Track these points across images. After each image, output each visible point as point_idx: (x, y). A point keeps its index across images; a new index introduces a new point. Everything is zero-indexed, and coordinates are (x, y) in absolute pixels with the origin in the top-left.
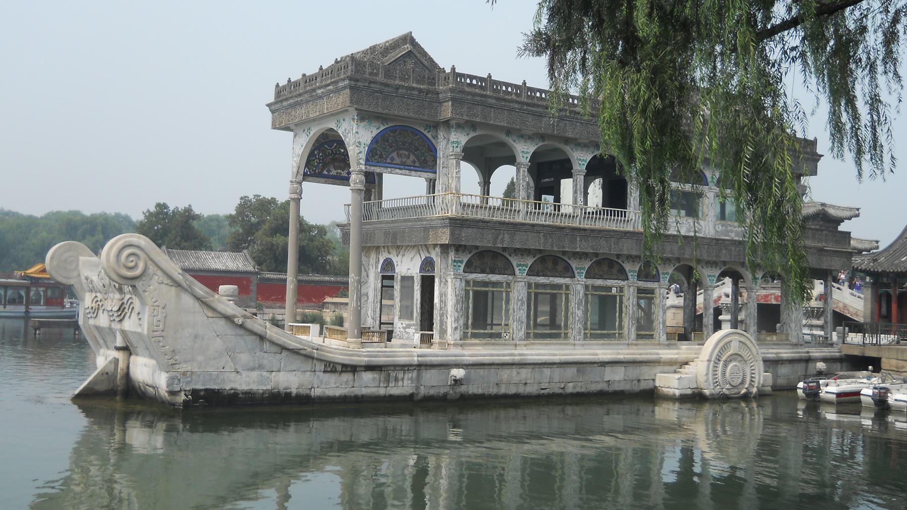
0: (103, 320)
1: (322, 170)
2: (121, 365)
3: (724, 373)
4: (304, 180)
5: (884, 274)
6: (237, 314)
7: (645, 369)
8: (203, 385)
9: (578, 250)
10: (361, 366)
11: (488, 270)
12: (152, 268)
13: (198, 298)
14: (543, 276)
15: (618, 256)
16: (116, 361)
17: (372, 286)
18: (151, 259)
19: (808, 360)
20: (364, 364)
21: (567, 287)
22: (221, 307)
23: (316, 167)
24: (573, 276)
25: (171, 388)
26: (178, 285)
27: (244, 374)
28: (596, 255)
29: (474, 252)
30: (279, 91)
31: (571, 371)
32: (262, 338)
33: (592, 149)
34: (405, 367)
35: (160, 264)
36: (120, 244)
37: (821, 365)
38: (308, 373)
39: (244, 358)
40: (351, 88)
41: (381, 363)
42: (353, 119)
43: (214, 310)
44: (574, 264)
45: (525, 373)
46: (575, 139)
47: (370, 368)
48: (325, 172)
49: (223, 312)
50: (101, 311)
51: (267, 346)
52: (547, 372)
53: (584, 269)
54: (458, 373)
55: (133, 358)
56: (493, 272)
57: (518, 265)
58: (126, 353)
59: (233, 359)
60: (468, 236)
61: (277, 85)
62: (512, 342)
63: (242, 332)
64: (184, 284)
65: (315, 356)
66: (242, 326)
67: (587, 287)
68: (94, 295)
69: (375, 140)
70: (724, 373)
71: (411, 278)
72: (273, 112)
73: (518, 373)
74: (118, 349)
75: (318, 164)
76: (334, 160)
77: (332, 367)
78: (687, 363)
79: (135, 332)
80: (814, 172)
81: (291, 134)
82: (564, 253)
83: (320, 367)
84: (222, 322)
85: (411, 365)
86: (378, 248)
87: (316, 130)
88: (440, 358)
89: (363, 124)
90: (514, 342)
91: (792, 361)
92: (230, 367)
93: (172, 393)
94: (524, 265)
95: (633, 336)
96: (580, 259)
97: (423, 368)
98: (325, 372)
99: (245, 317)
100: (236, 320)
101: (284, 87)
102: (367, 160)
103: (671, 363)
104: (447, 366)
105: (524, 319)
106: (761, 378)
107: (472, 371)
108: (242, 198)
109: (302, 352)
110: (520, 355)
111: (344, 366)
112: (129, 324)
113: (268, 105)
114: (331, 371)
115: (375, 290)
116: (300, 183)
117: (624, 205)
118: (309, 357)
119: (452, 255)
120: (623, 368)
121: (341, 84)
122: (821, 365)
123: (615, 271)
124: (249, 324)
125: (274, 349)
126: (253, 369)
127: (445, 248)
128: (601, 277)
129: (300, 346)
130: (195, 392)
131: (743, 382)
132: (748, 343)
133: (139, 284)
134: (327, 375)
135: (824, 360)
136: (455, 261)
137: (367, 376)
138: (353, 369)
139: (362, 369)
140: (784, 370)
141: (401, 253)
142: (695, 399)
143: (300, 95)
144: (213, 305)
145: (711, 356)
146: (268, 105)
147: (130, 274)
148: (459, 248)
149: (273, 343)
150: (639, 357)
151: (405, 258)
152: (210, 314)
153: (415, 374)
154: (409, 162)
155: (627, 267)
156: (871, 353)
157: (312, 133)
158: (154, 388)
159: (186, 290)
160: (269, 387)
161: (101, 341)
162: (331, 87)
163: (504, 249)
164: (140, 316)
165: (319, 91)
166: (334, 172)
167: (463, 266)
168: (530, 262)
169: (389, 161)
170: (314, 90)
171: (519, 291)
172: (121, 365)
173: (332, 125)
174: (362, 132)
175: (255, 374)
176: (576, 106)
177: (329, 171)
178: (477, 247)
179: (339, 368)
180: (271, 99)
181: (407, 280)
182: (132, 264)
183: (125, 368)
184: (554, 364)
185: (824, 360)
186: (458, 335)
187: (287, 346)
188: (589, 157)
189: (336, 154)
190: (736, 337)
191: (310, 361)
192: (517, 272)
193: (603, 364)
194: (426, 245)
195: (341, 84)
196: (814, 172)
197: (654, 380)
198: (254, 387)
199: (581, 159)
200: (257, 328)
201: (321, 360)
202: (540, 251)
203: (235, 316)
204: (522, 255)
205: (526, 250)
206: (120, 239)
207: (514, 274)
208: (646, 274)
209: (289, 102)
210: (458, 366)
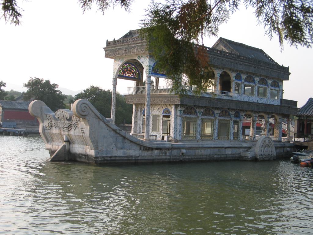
0: (55, 131)
1: (123, 74)
2: (67, 148)
3: (264, 151)
4: (118, 78)
5: (303, 116)
6: (117, 129)
7: (237, 150)
8: (106, 154)
10: (154, 148)
11: (189, 114)
12: (91, 112)
13: (105, 123)
14: (206, 116)
15: (229, 109)
16: (65, 146)
17: (139, 118)
18: (90, 109)
19: (284, 147)
20: (155, 147)
22: (112, 127)
23: (121, 73)
25: (96, 156)
26: (99, 118)
27: (119, 150)
28: (222, 108)
29: (186, 107)
30: (108, 43)
31: (216, 150)
32: (124, 138)
33: (221, 69)
34: (168, 149)
35: (93, 110)
36: (81, 103)
37: (288, 149)
38: (138, 151)
39: (119, 145)
40: (149, 45)
41: (161, 147)
42: (147, 57)
43: (110, 127)
45: (203, 150)
46: (217, 66)
47: (157, 149)
48: (124, 75)
49: (113, 128)
50: (54, 128)
51: (126, 141)
52: (209, 150)
54: (184, 151)
55: (71, 146)
56: (191, 114)
57: (199, 112)
58: (69, 143)
59: (115, 145)
60: (186, 102)
61: (107, 41)
62: (196, 140)
63: (118, 135)
64: (101, 119)
65: (141, 144)
66: (118, 133)
67: (219, 120)
68: (49, 121)
69: (154, 65)
70: (264, 151)
71: (159, 116)
72: (106, 51)
73: (201, 151)
74: (65, 141)
75: (122, 72)
76: (127, 70)
77: (146, 149)
78: (250, 148)
79: (78, 135)
80: (288, 79)
81: (112, 60)
83: (142, 148)
84: (113, 132)
85: (170, 148)
86: (142, 104)
87: (125, 60)
88: (178, 146)
89: (150, 59)
90: (197, 140)
91: (280, 147)
92: (115, 148)
93: (96, 157)
94: (200, 112)
95: (232, 138)
96: (217, 110)
97: (173, 149)
98: (143, 150)
99: (119, 130)
100: (117, 131)
101: (111, 42)
102: (152, 73)
103: (245, 148)
104: (179, 148)
106: (274, 153)
107: (187, 150)
108: (31, 78)
109: (137, 143)
110: (202, 145)
111: (149, 148)
112: (72, 132)
113: (103, 48)
114: (144, 150)
115: (140, 120)
116: (116, 79)
117: (229, 90)
118: (138, 144)
119: (179, 108)
120: (231, 150)
121: (144, 44)
122: (288, 149)
123: (227, 114)
124: (121, 133)
125: (129, 142)
126: (122, 149)
127: (176, 106)
128: (223, 117)
129: (137, 141)
130: (103, 157)
131: (269, 154)
132: (271, 141)
133: (87, 118)
134: (144, 151)
135: (289, 147)
136: (180, 110)
137: (156, 152)
138: (151, 149)
139: (155, 149)
140: (278, 151)
141: (153, 106)
142: (255, 160)
143: (122, 46)
144: (110, 126)
145: (260, 146)
146: (103, 48)
147: (84, 114)
148: (182, 105)
149: (128, 139)
150: (236, 146)
151: (155, 109)
152: (109, 129)
153: (170, 151)
154: (164, 73)
155: (231, 113)
156: (306, 144)
157: (124, 61)
158: (85, 155)
159: (101, 120)
160: (126, 155)
161: (50, 139)
162: (139, 44)
163: (195, 106)
164: (83, 129)
165: (133, 45)
166: (127, 75)
167: (182, 112)
169: (158, 72)
170: (130, 44)
171: (199, 122)
172: (67, 148)
173: (137, 59)
174: (151, 62)
175: (122, 151)
176: (218, 53)
177: (126, 74)
178: (187, 105)
179: (148, 148)
180: (105, 46)
181: (156, 117)
182: (84, 111)
183: (68, 149)
185: (289, 147)
186: (180, 138)
187: (132, 140)
188: (220, 72)
189: (128, 68)
190: (267, 139)
191: (139, 146)
192: (198, 115)
193: (226, 148)
194: (165, 104)
195: (144, 44)
196: (288, 79)
197: (240, 154)
198: (121, 155)
199: (218, 73)
200: (123, 134)
201: (142, 146)
202: (205, 107)
203: (117, 130)
204: (200, 108)
206: (80, 101)
207: (197, 114)
208: (237, 116)
209: (112, 49)
210: (183, 148)
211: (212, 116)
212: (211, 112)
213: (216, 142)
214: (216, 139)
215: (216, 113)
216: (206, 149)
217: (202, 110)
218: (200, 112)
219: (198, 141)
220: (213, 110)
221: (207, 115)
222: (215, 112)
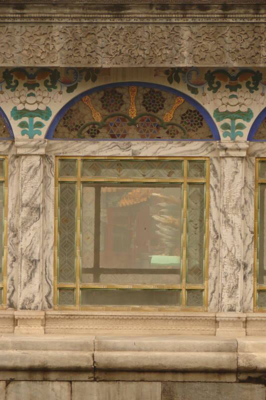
9: (186, 63)
14: (113, 137)
21: (198, 165)
24: (214, 136)
44: (211, 102)
53: (247, 115)
57: (18, 114)
62: (10, 312)
82: (174, 74)
94: (31, 114)
96: (233, 88)
105: (50, 257)
168: (56, 101)
184: (78, 370)
204: (31, 86)
205: (43, 71)
211: (173, 133)
212: (168, 116)
213: (250, 329)
214: (226, 302)
215: (221, 115)
216: (20, 376)
217: (56, 101)
218: (31, 114)
219: (15, 321)
220: (182, 88)
221: (132, 130)
222: (211, 102)
